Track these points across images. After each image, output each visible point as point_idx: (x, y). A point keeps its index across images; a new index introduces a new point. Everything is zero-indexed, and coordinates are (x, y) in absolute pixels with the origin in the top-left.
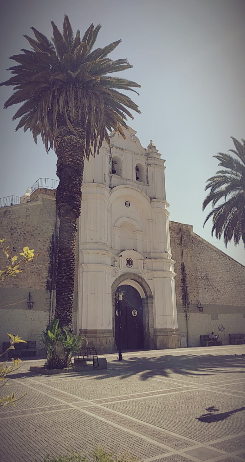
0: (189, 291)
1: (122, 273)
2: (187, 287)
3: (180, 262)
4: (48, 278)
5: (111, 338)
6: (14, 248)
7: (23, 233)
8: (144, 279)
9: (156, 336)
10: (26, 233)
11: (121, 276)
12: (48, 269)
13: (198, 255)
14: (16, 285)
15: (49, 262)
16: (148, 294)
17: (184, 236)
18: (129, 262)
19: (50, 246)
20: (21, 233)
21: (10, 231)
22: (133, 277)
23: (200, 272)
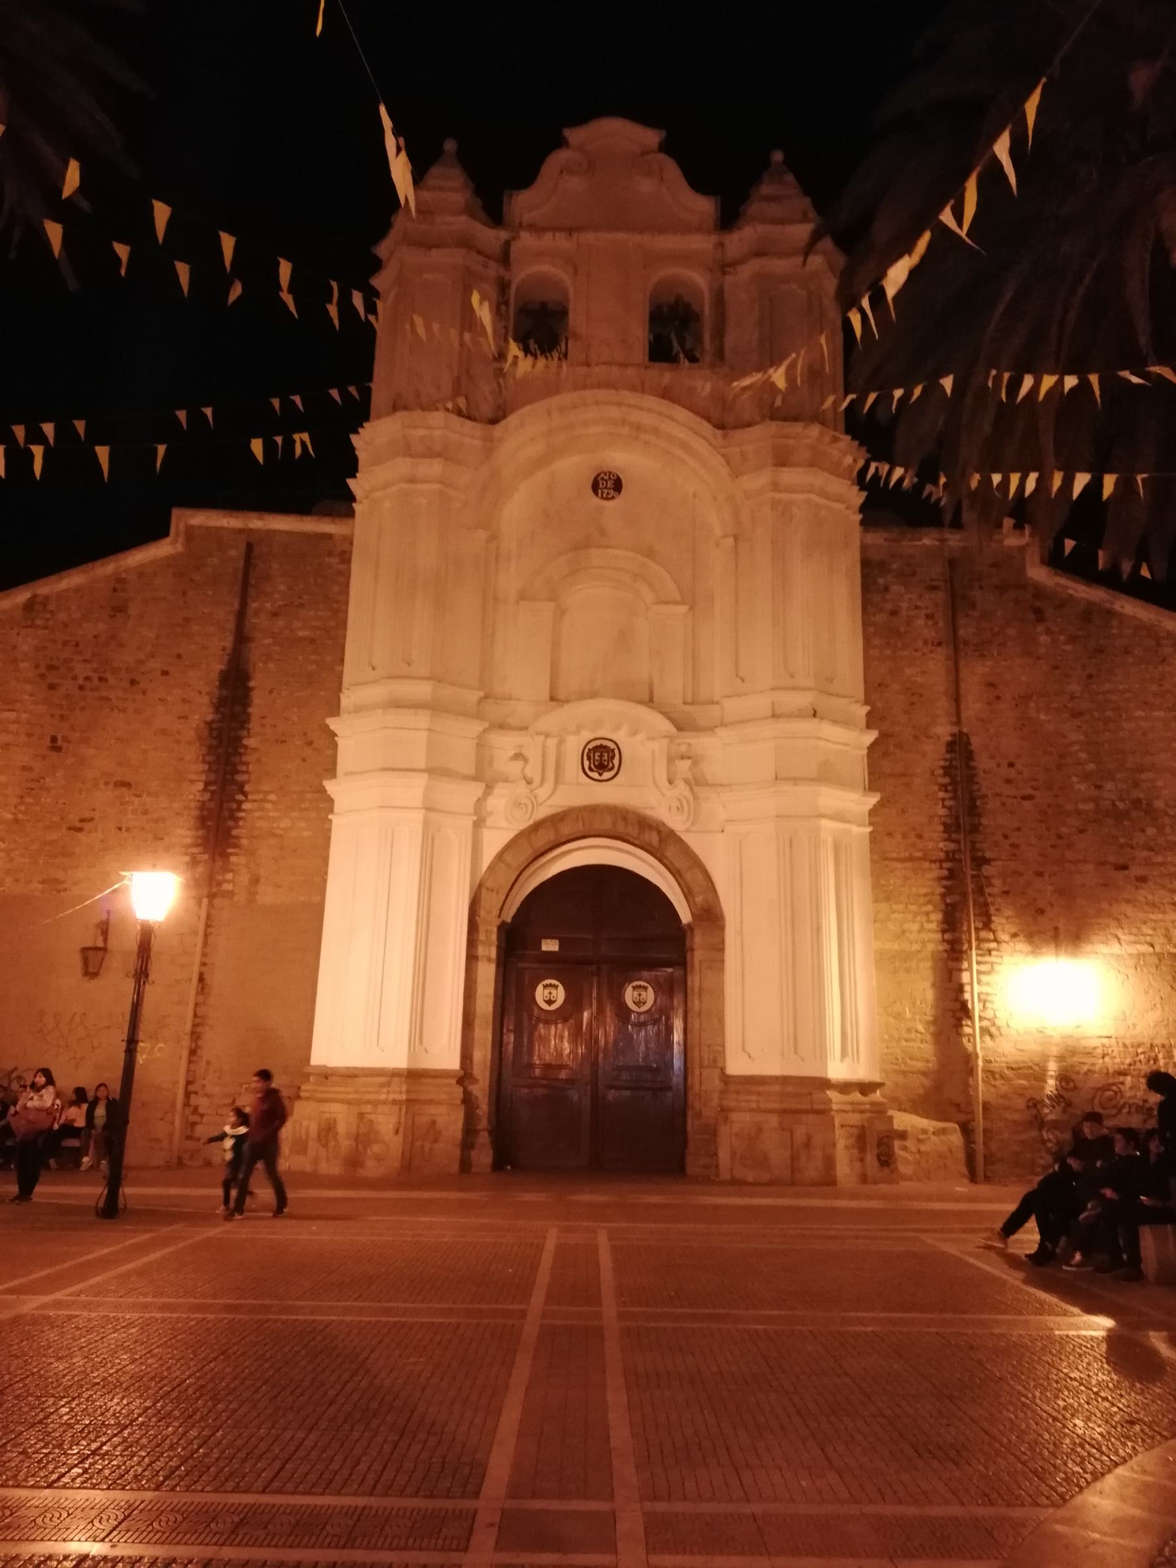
0: (997, 882)
1: (541, 813)
2: (987, 861)
3: (944, 731)
4: (194, 850)
5: (442, 1110)
6: (54, 739)
7: (95, 677)
8: (672, 833)
9: (725, 1111)
10: (108, 676)
11: (537, 826)
12: (195, 813)
13: (1075, 687)
14: (57, 881)
15: (201, 786)
16: (699, 899)
17: (976, 594)
18: (602, 759)
19: (210, 718)
20: (87, 678)
21: (42, 676)
22: (607, 824)
23: (1085, 777)
